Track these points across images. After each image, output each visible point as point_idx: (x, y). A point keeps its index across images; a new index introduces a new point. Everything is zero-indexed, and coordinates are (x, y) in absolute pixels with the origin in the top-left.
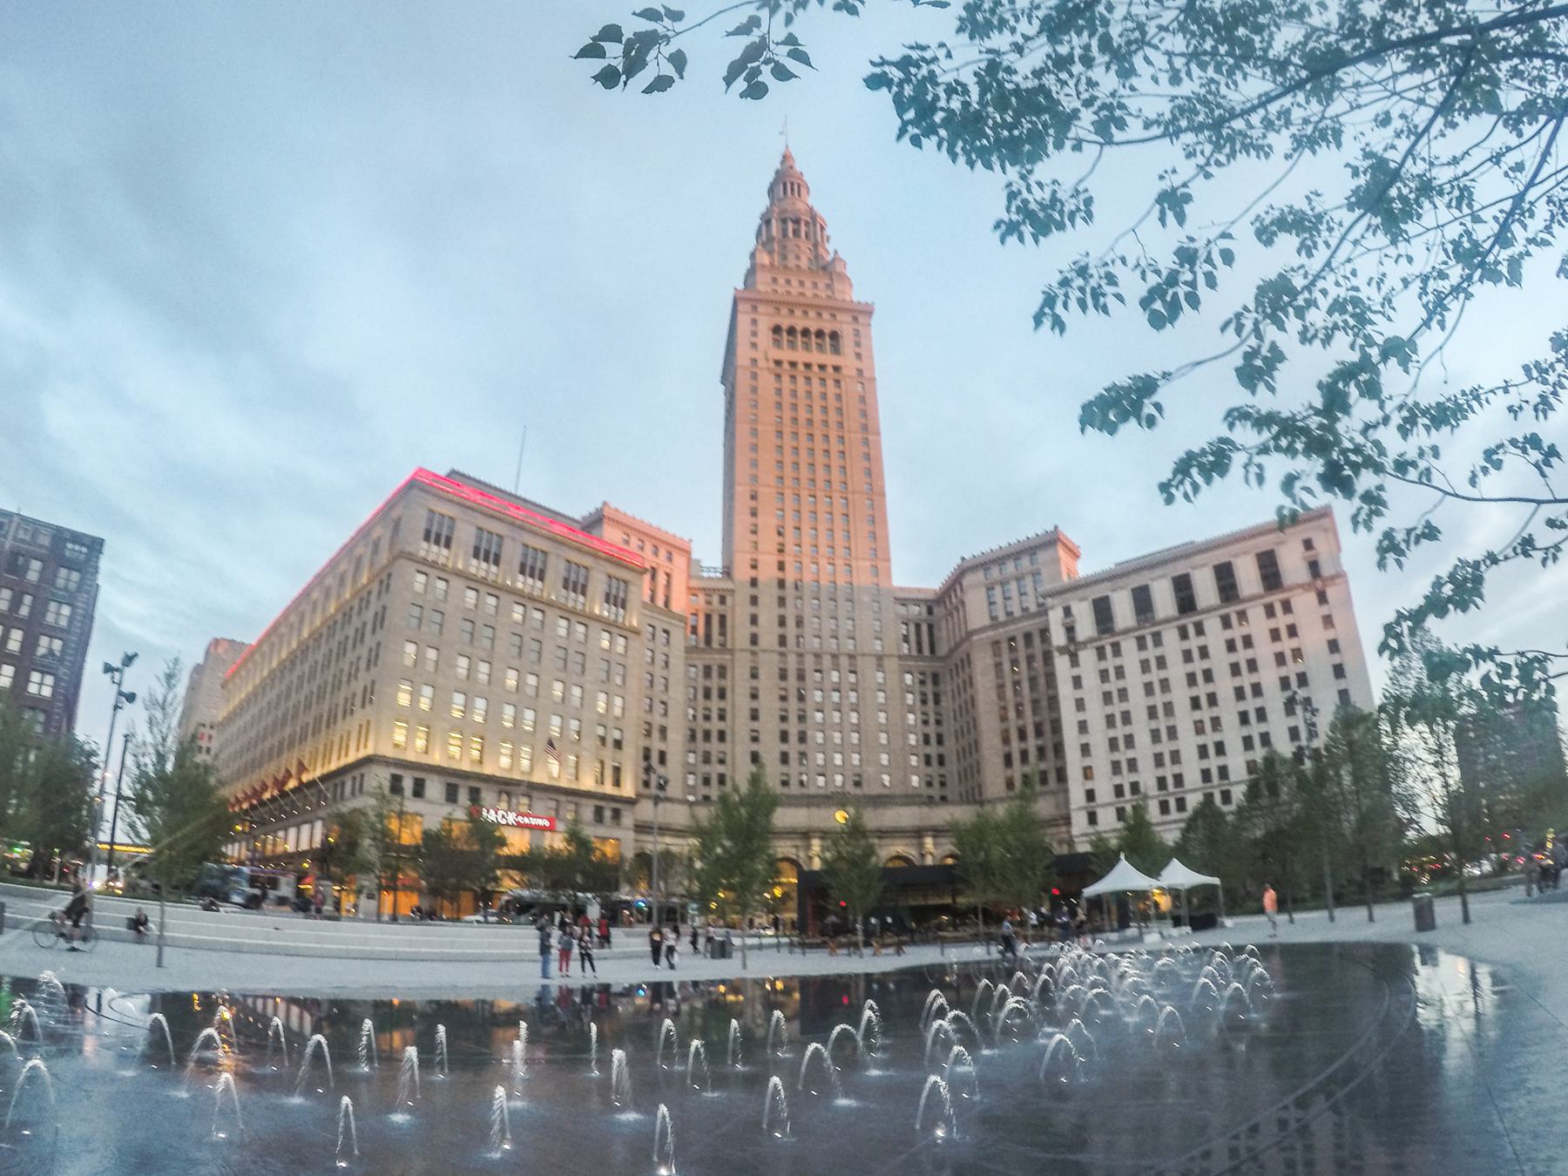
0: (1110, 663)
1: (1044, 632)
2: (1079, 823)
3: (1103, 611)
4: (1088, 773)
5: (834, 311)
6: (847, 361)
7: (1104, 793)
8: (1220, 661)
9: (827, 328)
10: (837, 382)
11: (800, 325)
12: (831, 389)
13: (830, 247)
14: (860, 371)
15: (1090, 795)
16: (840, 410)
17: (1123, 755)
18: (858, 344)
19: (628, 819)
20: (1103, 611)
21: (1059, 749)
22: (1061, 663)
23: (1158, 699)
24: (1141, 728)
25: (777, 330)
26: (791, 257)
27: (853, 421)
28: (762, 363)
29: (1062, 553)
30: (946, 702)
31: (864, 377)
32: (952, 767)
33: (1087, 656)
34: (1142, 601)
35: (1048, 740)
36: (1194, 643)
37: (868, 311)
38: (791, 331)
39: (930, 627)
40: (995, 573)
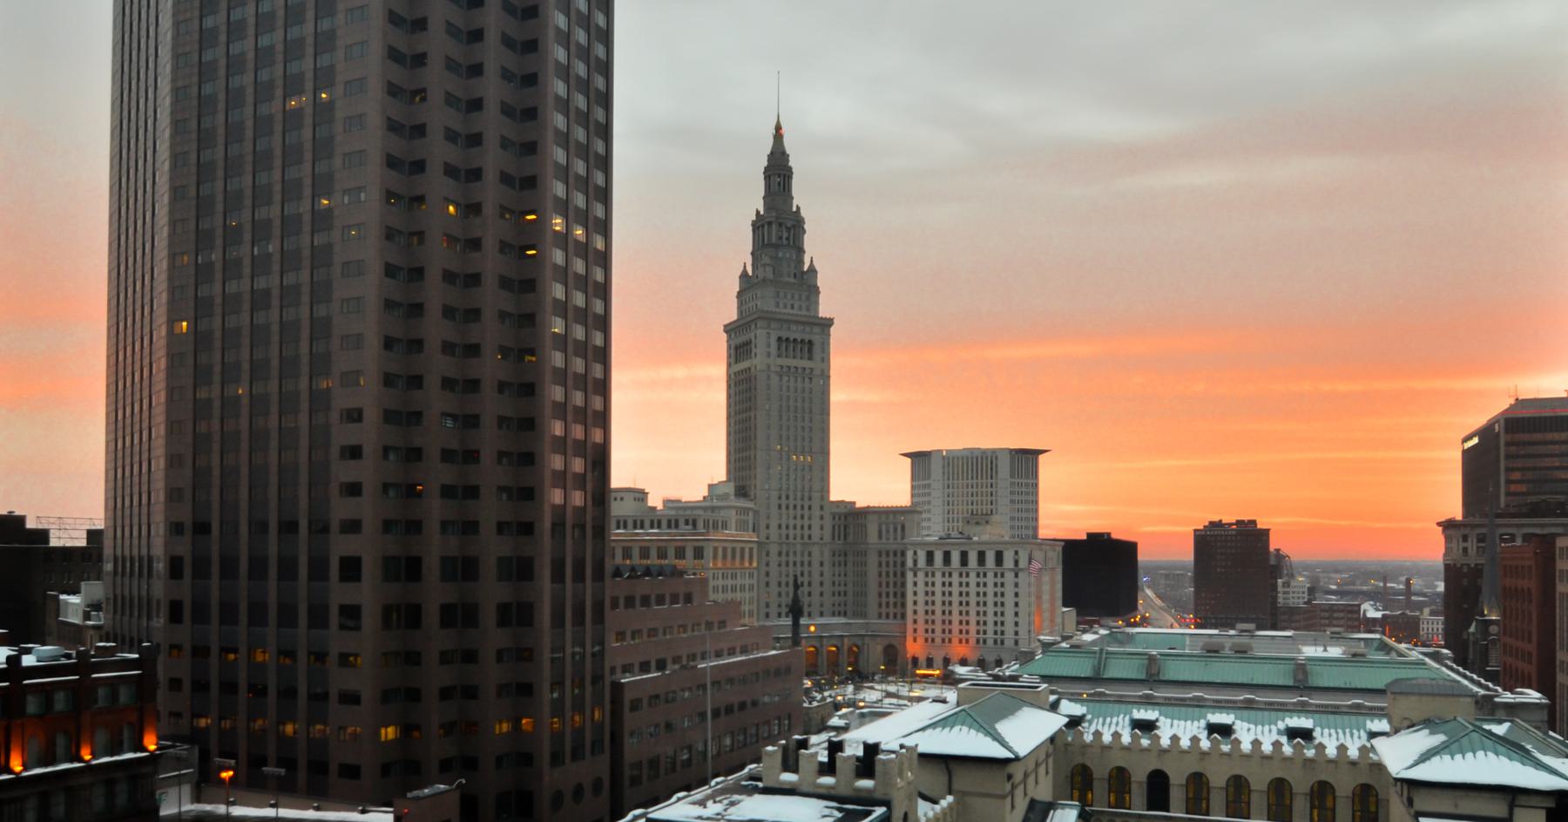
0: (930, 580)
1: (903, 554)
3: (930, 557)
4: (915, 622)
7: (921, 631)
8: (973, 589)
9: (807, 338)
12: (807, 385)
17: (930, 617)
20: (930, 557)
21: (903, 605)
22: (910, 575)
24: (938, 608)
25: (780, 339)
30: (850, 565)
31: (826, 377)
32: (850, 598)
33: (921, 575)
35: (899, 600)
36: (964, 580)
37: (828, 323)
40: (884, 518)
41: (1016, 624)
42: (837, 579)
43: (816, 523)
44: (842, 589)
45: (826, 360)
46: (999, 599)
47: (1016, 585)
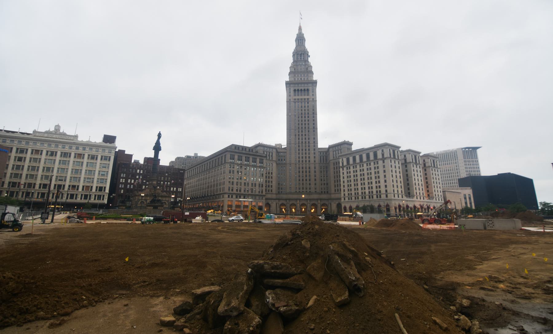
0: (348, 171)
2: (343, 199)
4: (344, 191)
5: (308, 83)
6: (310, 97)
7: (347, 195)
8: (365, 172)
9: (306, 88)
10: (308, 103)
11: (300, 89)
12: (306, 105)
13: (310, 60)
14: (313, 99)
15: (344, 195)
16: (308, 110)
18: (313, 92)
19: (264, 198)
23: (355, 178)
25: (295, 90)
26: (299, 66)
27: (311, 113)
28: (292, 100)
29: (346, 146)
31: (314, 101)
33: (345, 169)
34: (354, 159)
37: (315, 83)
38: (298, 90)
39: (326, 157)
40: (334, 149)
41: (386, 186)
42: (322, 178)
43: (312, 156)
44: (325, 182)
45: (314, 94)
46: (377, 175)
47: (384, 166)
